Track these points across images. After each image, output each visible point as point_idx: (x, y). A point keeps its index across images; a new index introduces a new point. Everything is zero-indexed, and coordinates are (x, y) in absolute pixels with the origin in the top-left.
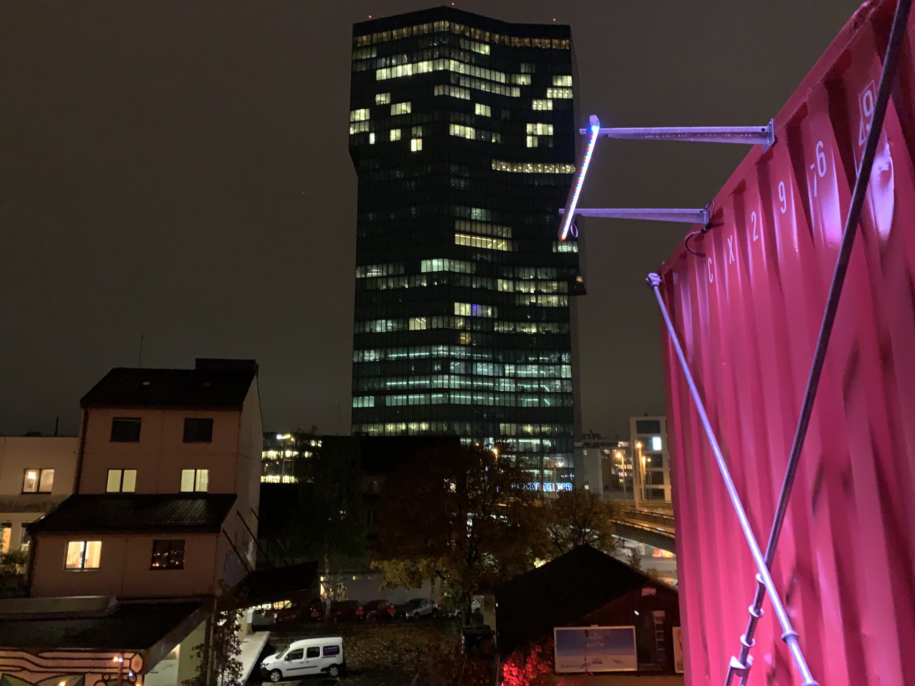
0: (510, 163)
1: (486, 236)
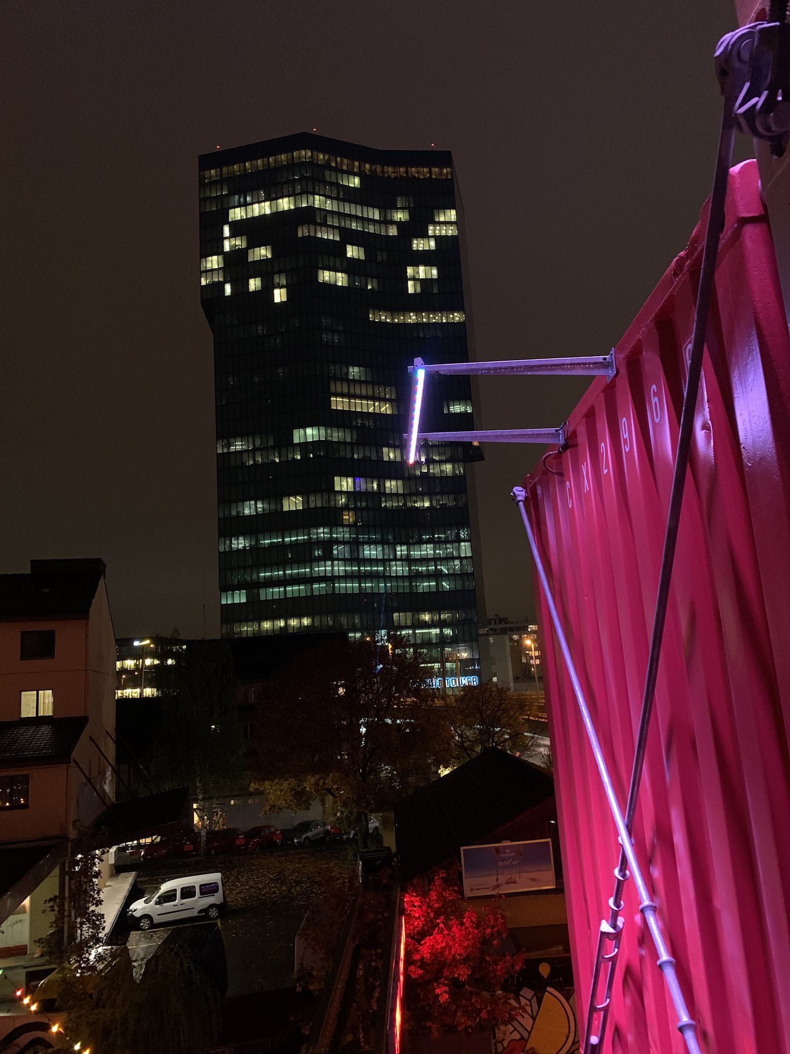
1: (367, 398)
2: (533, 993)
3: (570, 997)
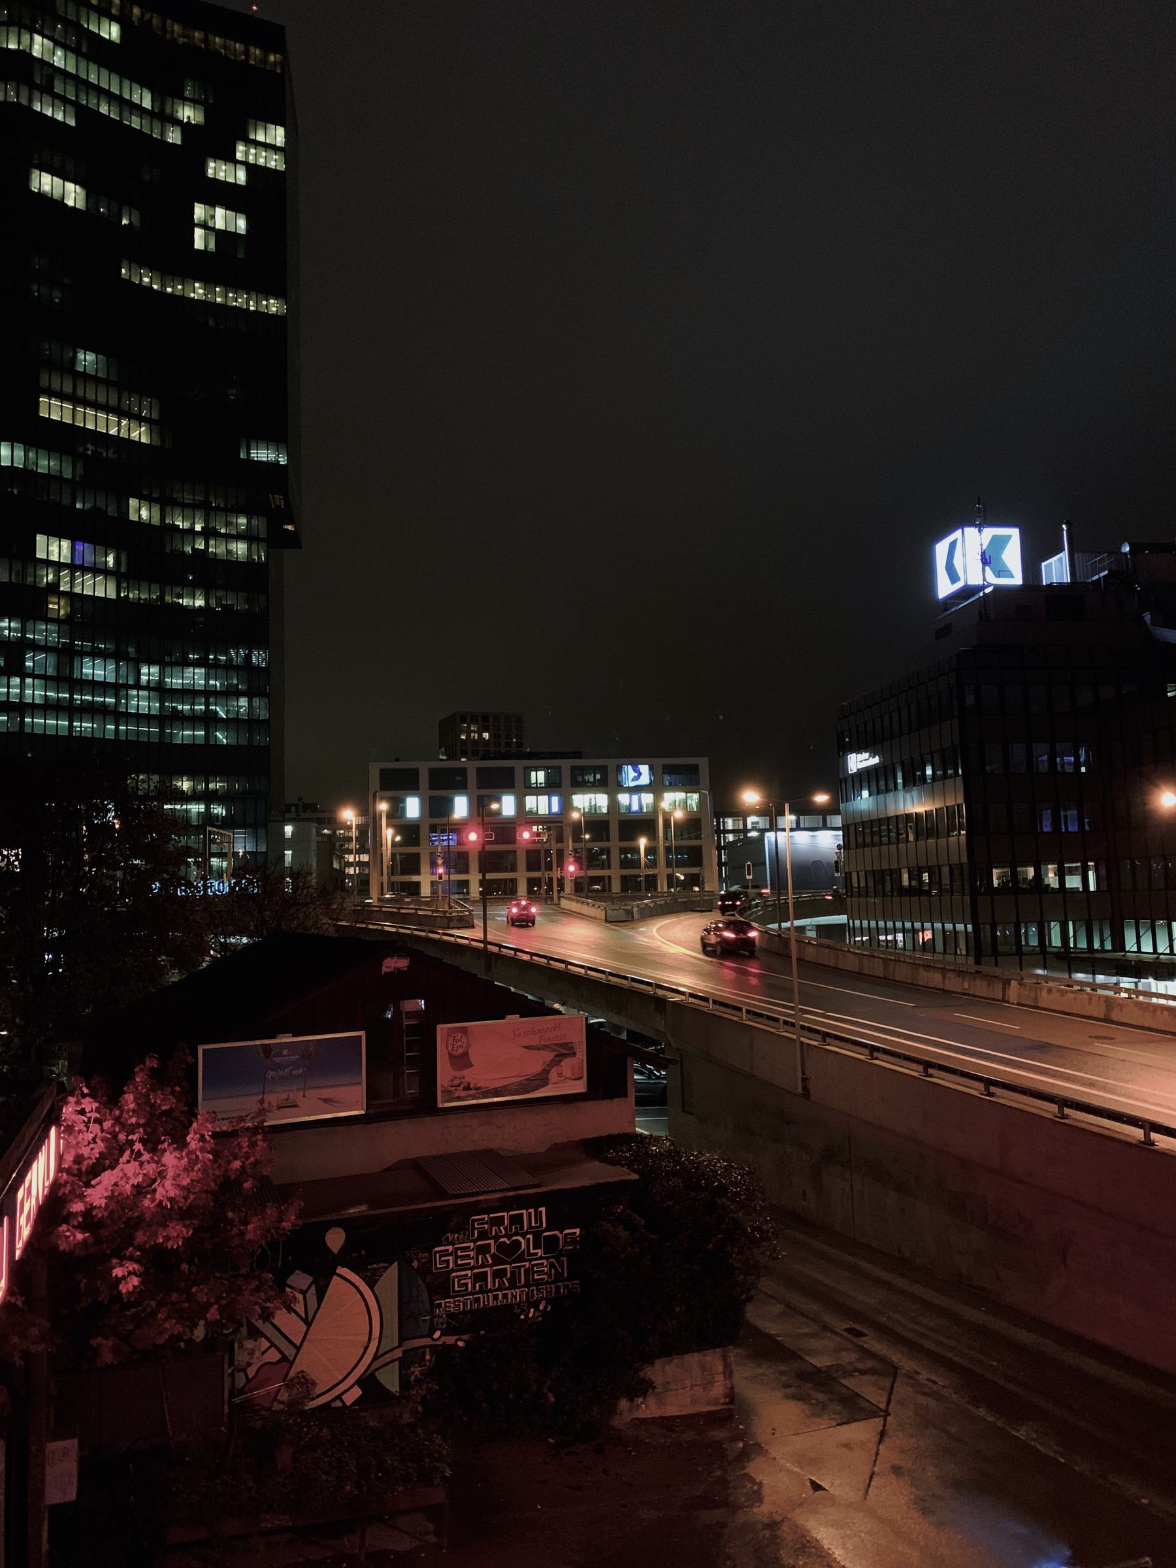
0: (158, 273)
1: (107, 409)
2: (311, 1279)
3: (376, 1281)
